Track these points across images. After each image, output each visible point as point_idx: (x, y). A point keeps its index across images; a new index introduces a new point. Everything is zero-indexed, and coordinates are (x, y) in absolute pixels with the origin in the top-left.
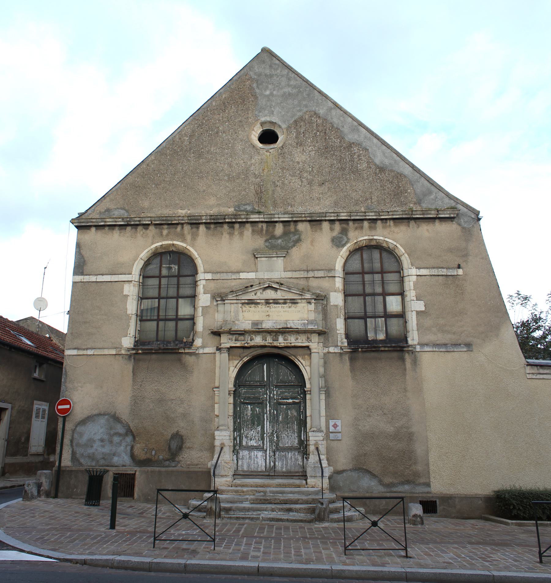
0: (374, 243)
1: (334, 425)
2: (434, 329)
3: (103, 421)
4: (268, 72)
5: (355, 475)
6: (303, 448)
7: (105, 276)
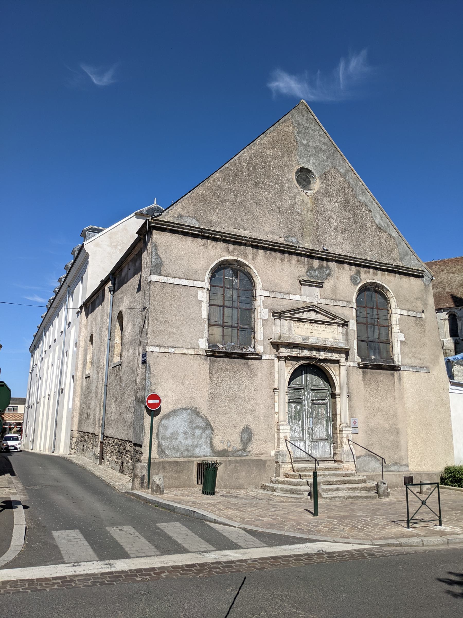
2: (410, 355)
3: (185, 415)
4: (305, 123)
5: (366, 459)
6: (333, 439)
7: (181, 280)
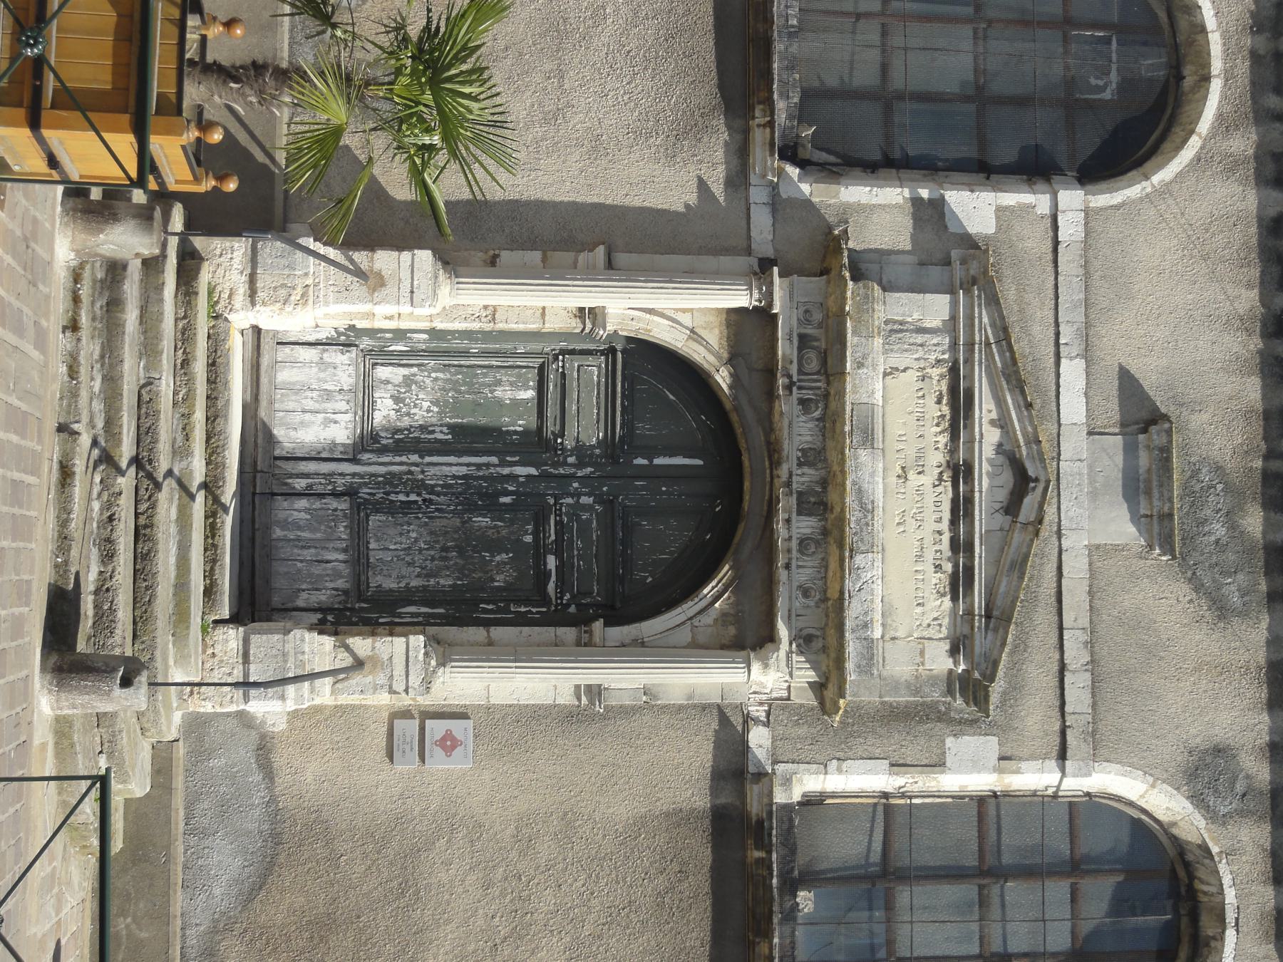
0: (1208, 929)
1: (454, 739)
5: (253, 820)
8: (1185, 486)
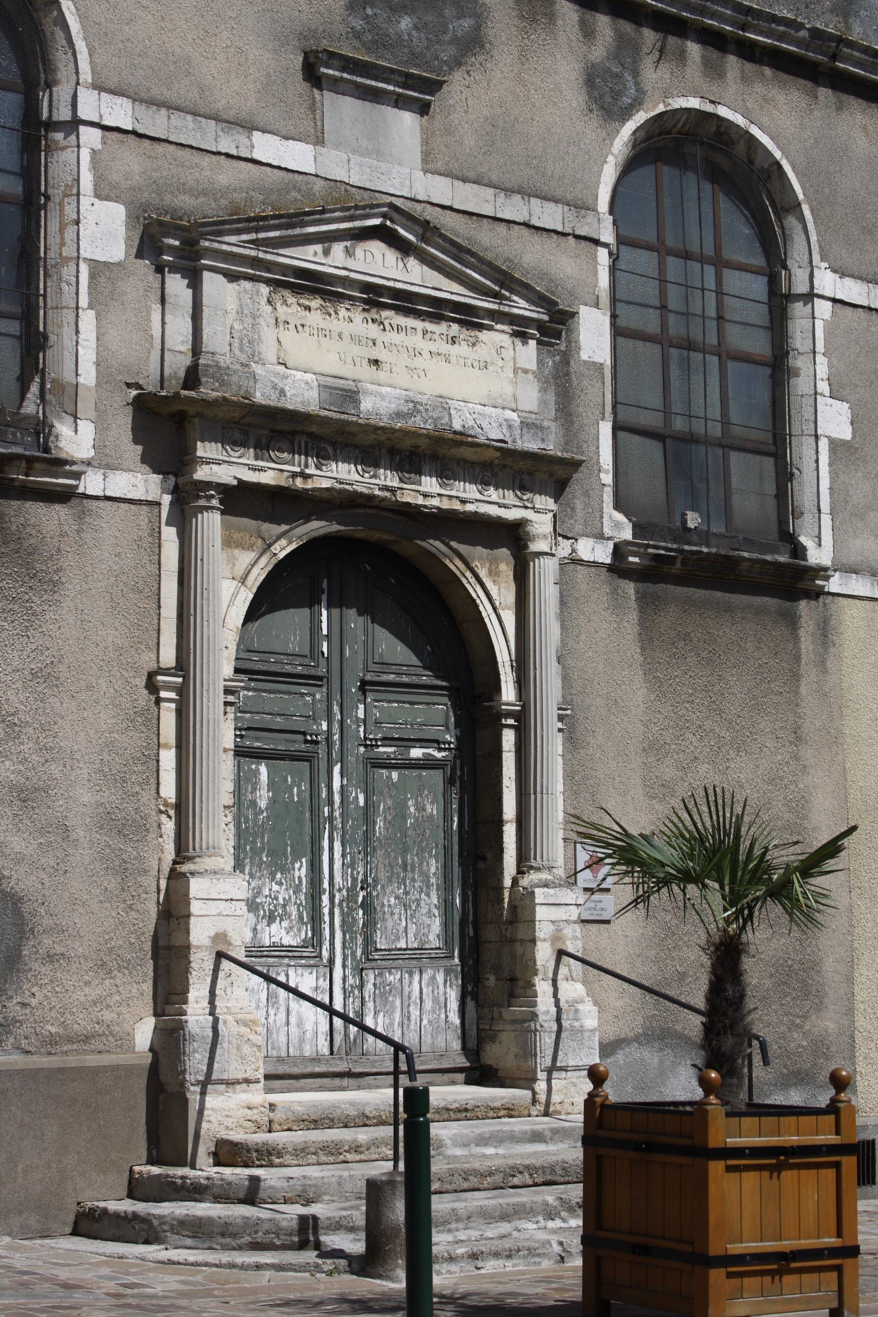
8: (369, 51)
